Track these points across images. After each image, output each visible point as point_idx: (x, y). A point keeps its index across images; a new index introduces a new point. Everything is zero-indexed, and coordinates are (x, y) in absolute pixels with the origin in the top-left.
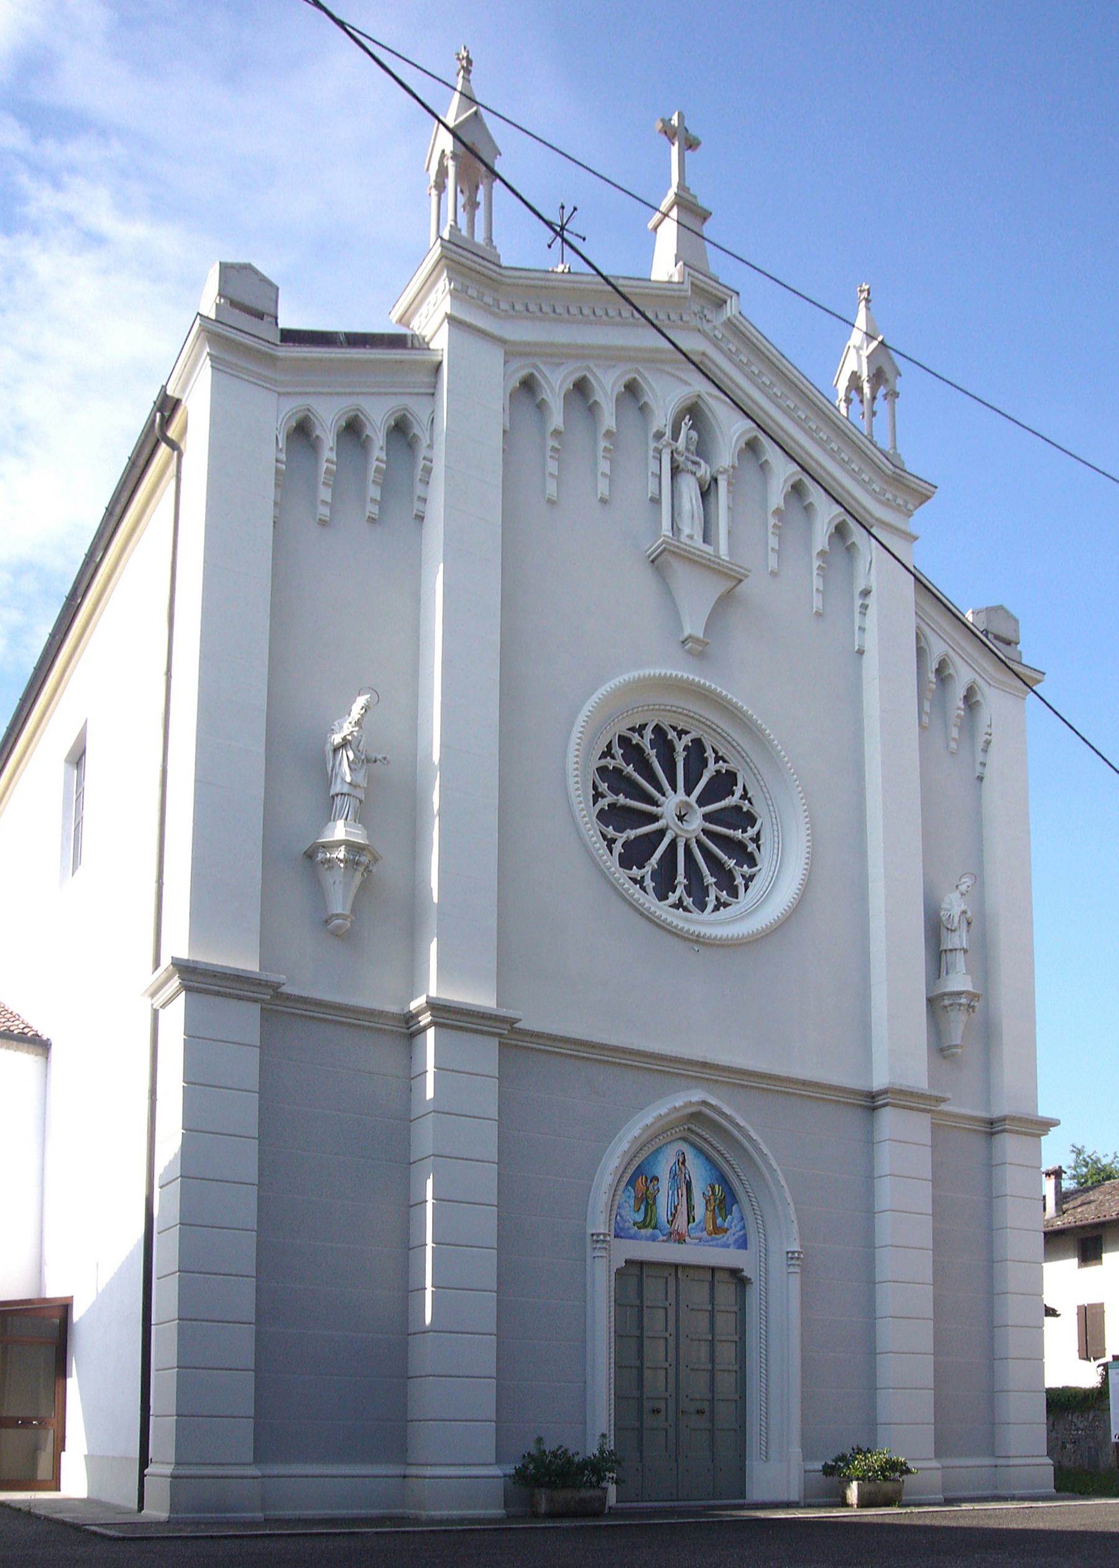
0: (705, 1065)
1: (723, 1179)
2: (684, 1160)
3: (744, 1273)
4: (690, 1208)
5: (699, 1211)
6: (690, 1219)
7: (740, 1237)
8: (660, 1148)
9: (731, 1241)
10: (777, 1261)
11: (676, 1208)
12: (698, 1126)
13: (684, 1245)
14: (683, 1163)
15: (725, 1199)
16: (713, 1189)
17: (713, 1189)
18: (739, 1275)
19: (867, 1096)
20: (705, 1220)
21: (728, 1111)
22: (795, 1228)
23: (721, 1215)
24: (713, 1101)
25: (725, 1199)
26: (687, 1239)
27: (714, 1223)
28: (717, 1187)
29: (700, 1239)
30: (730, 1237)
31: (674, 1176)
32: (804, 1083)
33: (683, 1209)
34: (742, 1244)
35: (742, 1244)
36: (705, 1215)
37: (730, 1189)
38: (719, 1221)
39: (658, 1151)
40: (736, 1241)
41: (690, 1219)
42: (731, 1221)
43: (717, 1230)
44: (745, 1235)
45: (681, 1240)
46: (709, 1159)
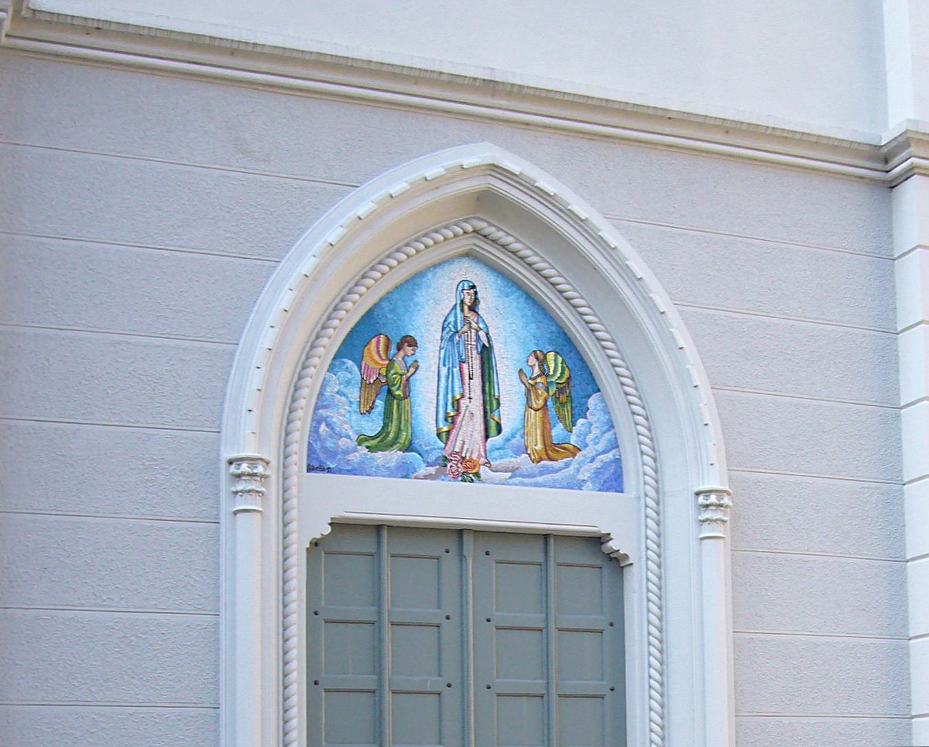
0: (491, 87)
1: (566, 343)
2: (476, 301)
3: (612, 545)
4: (490, 403)
5: (511, 411)
6: (491, 427)
7: (606, 465)
8: (420, 275)
9: (585, 475)
10: (680, 511)
11: (456, 404)
12: (493, 218)
13: (476, 485)
14: (473, 308)
15: (569, 385)
16: (542, 361)
17: (542, 361)
18: (605, 548)
19: (871, 158)
20: (524, 429)
21: (581, 208)
22: (713, 436)
23: (561, 418)
24: (513, 164)
25: (569, 385)
26: (484, 470)
27: (546, 435)
28: (551, 356)
29: (514, 471)
30: (583, 466)
31: (451, 335)
32: (727, 127)
33: (473, 406)
34: (613, 480)
35: (613, 480)
36: (525, 417)
37: (582, 360)
38: (558, 431)
39: (414, 281)
40: (597, 473)
41: (491, 427)
42: (586, 430)
43: (553, 450)
44: (618, 461)
45: (468, 472)
46: (531, 298)
